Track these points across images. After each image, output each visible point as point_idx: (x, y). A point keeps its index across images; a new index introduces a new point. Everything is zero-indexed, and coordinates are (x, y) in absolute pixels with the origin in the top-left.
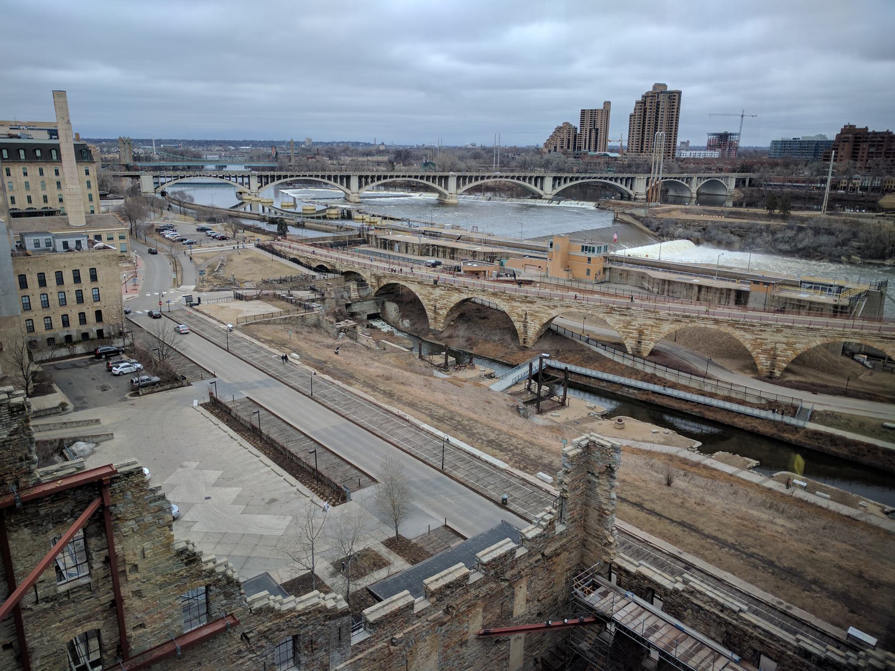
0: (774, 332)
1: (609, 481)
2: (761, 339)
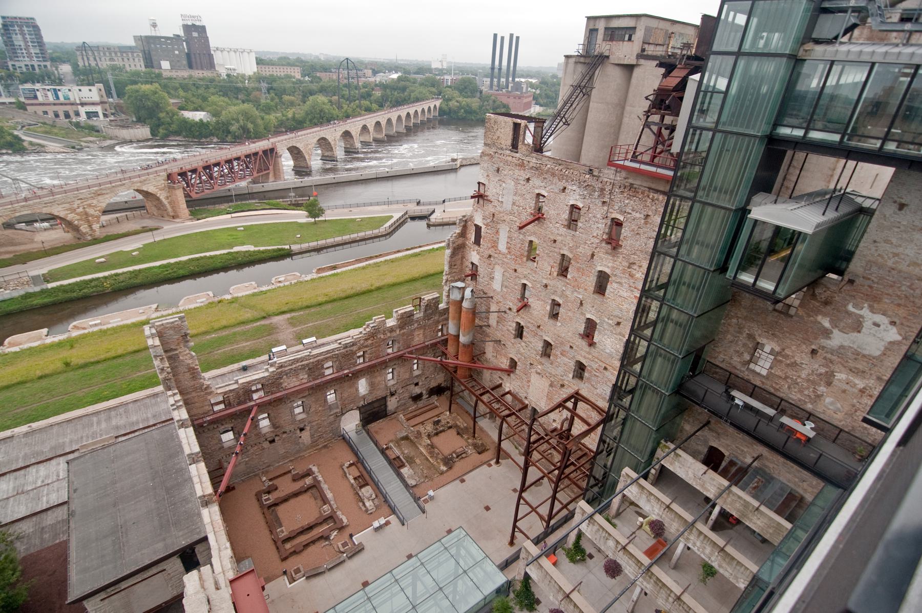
1: (184, 346)
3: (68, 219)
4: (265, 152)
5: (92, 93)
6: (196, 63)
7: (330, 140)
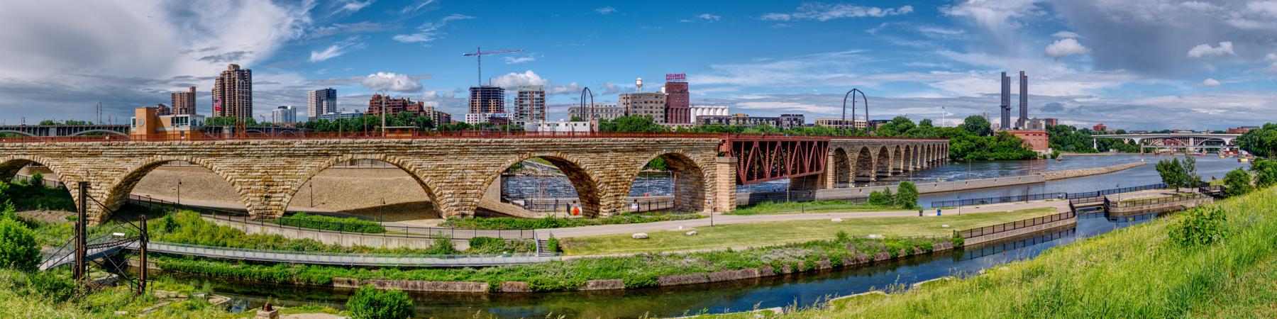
0: (459, 153)
6: (677, 116)
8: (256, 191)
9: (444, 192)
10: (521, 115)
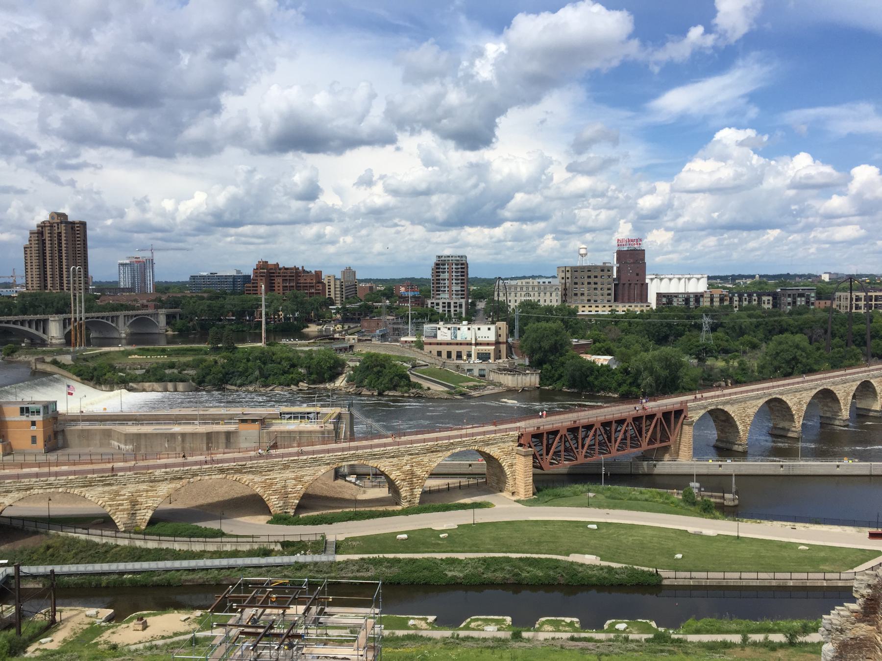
0: (282, 469)
2: (270, 479)
3: (392, 477)
4: (666, 415)
5: (486, 332)
7: (790, 404)
8: (124, 510)
9: (271, 497)
10: (437, 291)
